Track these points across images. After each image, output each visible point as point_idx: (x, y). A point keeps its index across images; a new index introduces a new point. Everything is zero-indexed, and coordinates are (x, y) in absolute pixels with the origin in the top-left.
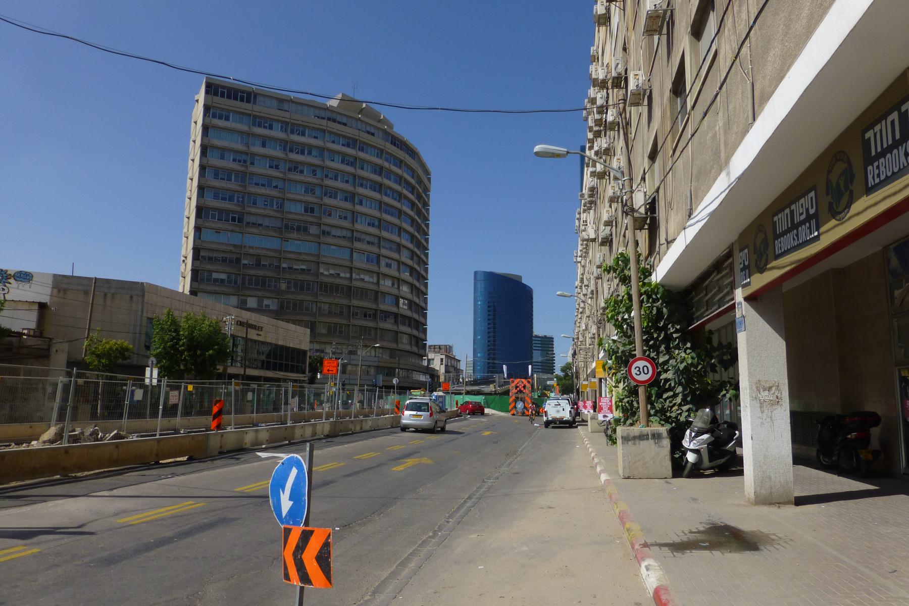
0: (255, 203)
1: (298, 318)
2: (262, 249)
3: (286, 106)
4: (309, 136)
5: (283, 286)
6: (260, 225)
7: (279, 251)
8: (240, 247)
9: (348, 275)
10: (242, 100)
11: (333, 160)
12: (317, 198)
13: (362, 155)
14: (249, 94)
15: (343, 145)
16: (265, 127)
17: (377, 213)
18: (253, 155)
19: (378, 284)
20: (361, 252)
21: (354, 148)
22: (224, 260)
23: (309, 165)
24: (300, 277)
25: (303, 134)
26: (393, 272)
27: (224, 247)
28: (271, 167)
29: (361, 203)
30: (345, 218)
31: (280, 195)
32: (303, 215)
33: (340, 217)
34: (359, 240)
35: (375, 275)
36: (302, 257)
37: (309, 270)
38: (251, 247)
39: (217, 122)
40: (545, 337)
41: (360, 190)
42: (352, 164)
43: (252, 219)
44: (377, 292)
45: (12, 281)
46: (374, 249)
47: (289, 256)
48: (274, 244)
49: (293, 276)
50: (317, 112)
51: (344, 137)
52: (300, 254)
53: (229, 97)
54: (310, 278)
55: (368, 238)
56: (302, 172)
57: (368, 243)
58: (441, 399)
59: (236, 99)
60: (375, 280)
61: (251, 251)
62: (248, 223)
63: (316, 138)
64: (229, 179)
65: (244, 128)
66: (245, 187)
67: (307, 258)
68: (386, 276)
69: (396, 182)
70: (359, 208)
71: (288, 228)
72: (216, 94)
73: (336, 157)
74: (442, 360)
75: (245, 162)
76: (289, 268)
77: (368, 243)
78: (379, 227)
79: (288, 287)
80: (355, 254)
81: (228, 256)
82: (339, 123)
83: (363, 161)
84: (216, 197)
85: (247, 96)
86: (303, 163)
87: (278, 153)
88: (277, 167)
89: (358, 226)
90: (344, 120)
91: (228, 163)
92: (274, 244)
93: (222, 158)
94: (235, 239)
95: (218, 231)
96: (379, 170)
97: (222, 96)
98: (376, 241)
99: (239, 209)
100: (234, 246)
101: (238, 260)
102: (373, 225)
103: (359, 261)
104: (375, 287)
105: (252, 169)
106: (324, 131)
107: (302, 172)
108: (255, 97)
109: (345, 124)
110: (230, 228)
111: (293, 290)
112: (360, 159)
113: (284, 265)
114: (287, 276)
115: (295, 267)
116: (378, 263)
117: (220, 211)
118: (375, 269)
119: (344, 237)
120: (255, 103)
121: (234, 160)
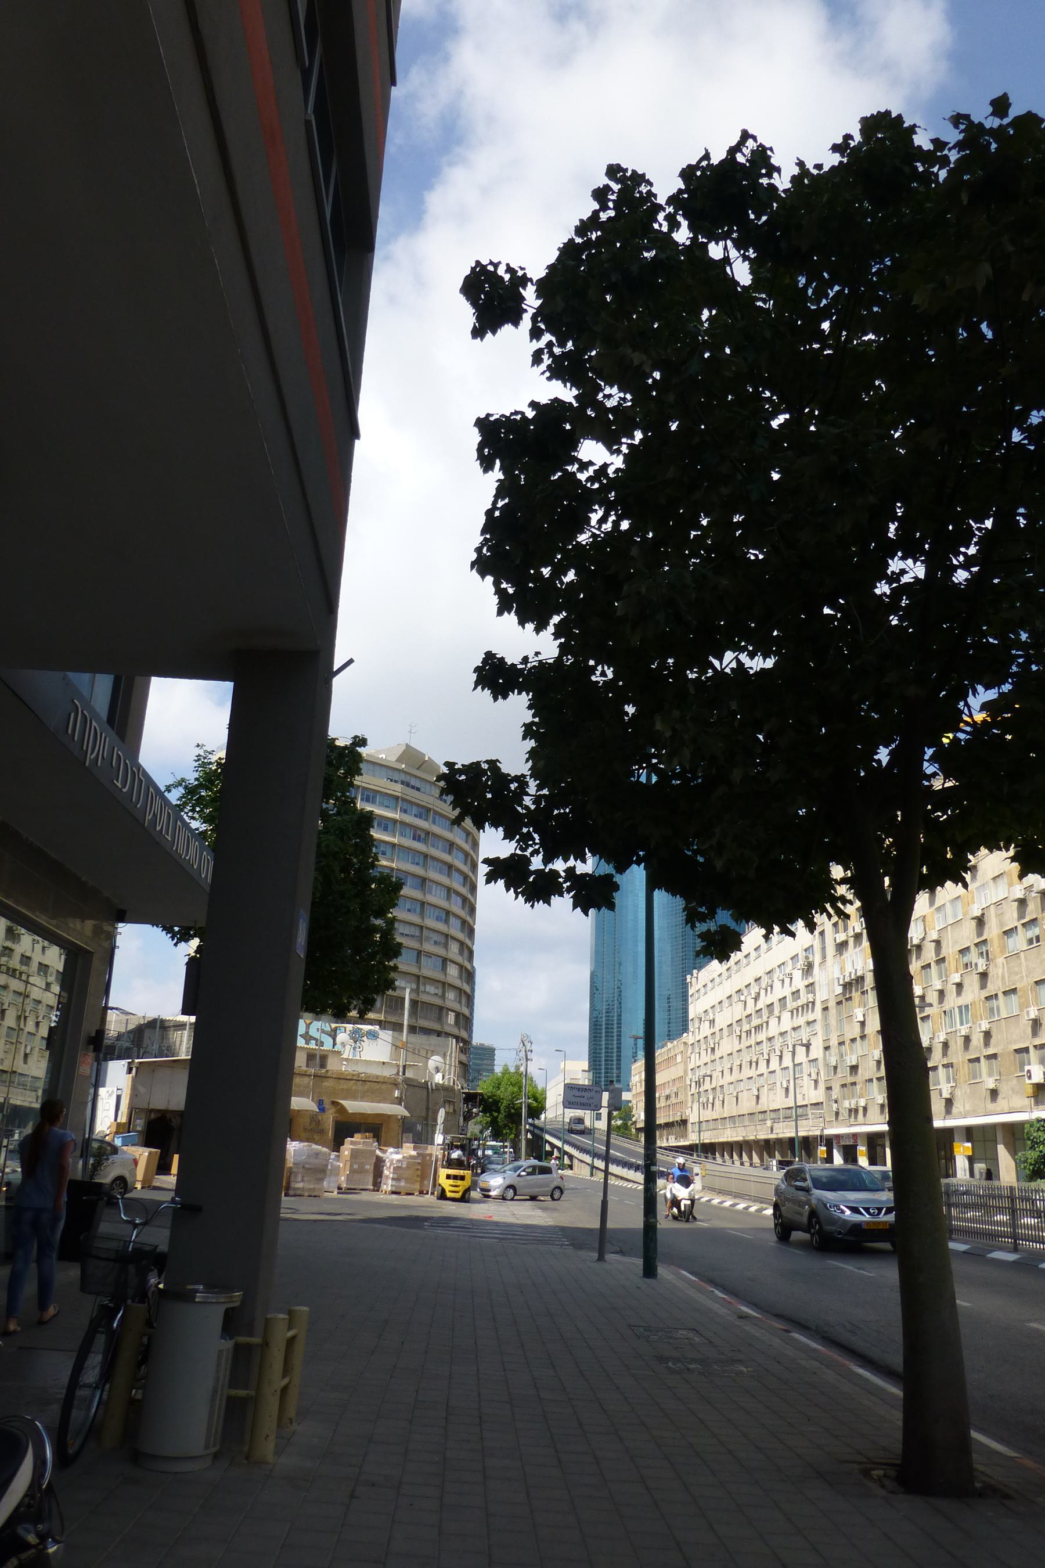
13: (436, 829)
15: (415, 816)
17: (444, 904)
19: (443, 997)
20: (429, 955)
21: (426, 820)
25: (374, 802)
26: (458, 983)
29: (430, 893)
30: (415, 911)
33: (409, 910)
34: (428, 939)
35: (440, 985)
41: (433, 875)
42: (425, 841)
44: (441, 1009)
45: (365, 1038)
46: (441, 951)
50: (390, 773)
51: (418, 805)
55: (435, 937)
57: (435, 943)
60: (440, 992)
68: (453, 987)
69: (444, 851)
70: (430, 898)
73: (408, 830)
77: (435, 943)
78: (447, 922)
82: (413, 787)
83: (435, 835)
89: (430, 922)
90: (418, 784)
96: (451, 846)
98: (441, 939)
102: (441, 920)
103: (429, 969)
104: (438, 1001)
106: (397, 798)
109: (418, 789)
112: (433, 834)
116: (444, 968)
118: (440, 977)
119: (413, 936)
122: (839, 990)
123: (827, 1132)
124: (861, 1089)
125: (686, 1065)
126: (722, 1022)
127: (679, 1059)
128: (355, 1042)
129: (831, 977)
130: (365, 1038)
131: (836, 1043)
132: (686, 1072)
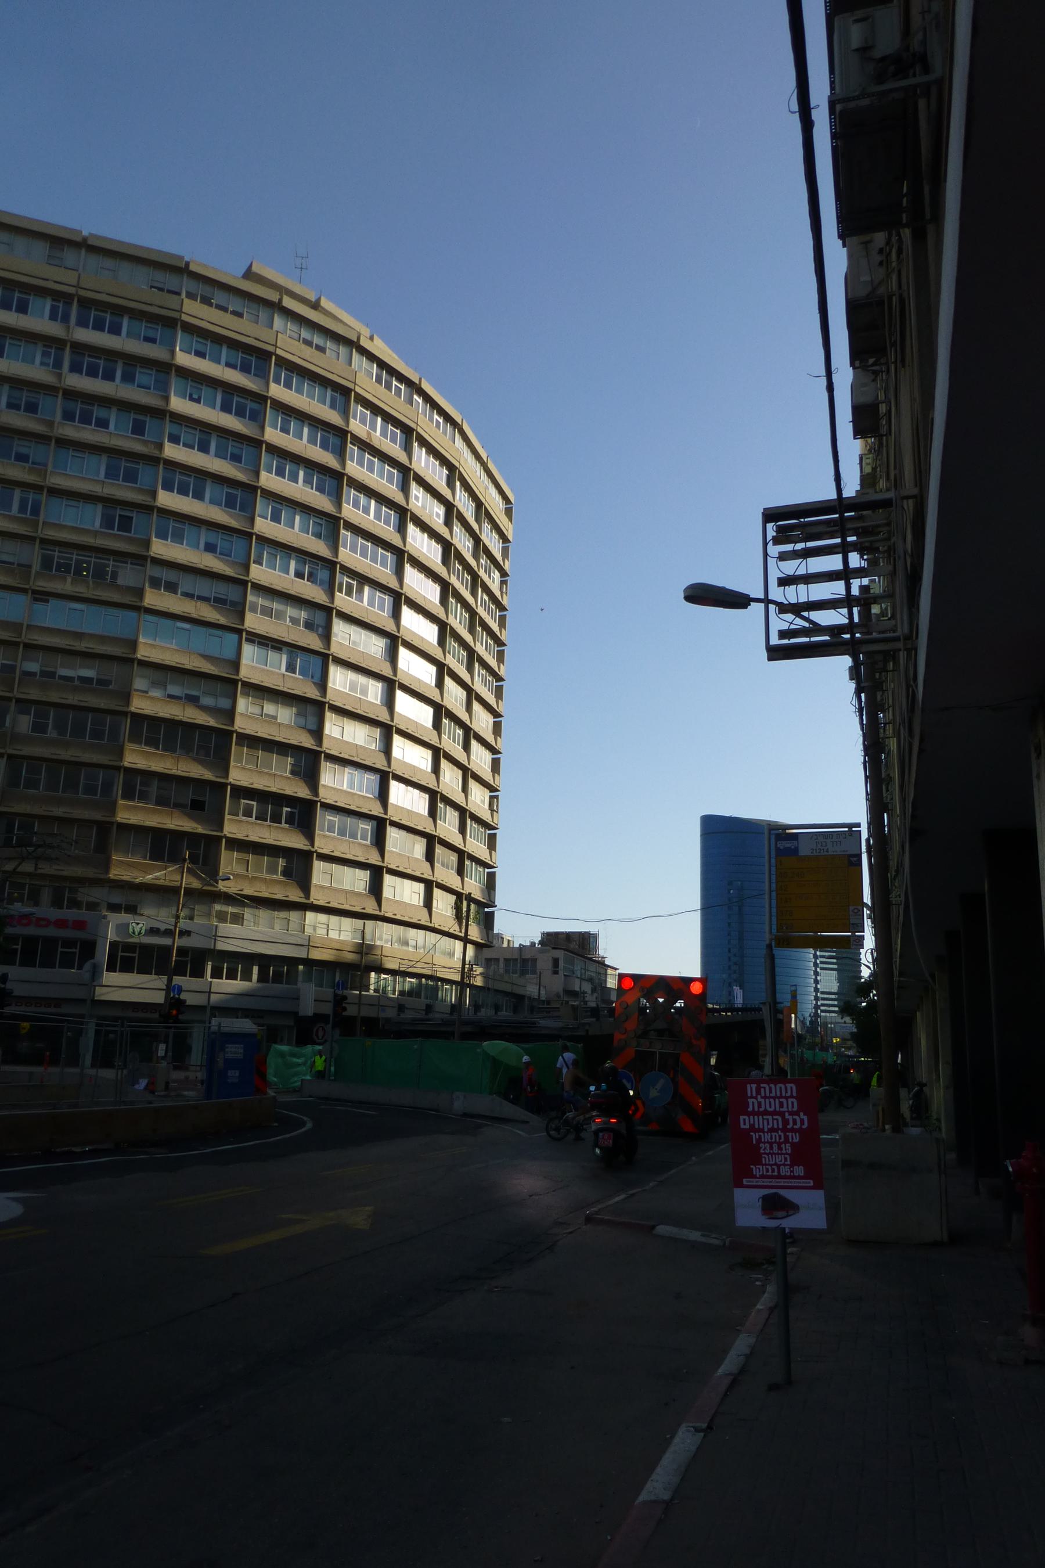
1: (59, 811)
3: (70, 257)
4: (129, 335)
5: (24, 723)
9: (224, 703)
11: (198, 401)
12: (140, 491)
15: (228, 365)
23: (125, 406)
24: (73, 699)
25: (115, 330)
28: (11, 406)
31: (31, 478)
36: (82, 646)
37: (100, 682)
49: (54, 697)
50: (160, 277)
51: (234, 345)
52: (79, 636)
54: (102, 703)
63: (152, 340)
73: (206, 391)
74: (556, 962)
79: (39, 727)
86: (106, 402)
87: (36, 371)
88: (32, 408)
107: (103, 424)
111: (51, 733)
113: (33, 667)
114: (34, 694)
115: (63, 672)
119: (217, 600)
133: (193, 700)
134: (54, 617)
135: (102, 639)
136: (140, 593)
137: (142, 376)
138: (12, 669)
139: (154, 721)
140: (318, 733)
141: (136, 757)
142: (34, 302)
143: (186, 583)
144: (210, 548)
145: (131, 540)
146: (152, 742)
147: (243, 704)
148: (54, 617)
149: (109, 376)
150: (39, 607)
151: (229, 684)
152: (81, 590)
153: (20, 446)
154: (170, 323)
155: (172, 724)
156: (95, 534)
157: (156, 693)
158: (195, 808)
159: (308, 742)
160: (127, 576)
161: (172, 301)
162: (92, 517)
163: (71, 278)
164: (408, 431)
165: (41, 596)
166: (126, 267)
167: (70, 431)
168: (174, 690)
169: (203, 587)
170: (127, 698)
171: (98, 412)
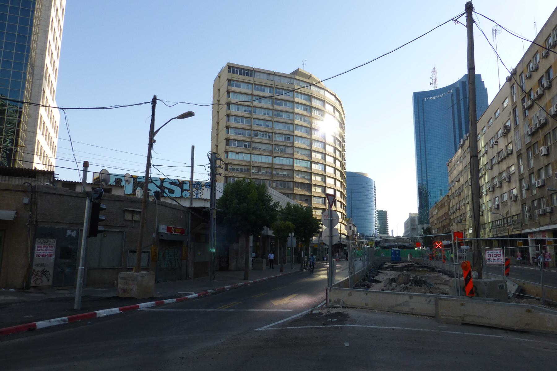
0: (257, 136)
2: (262, 163)
3: (271, 77)
6: (260, 149)
7: (272, 164)
8: (250, 162)
9: (309, 177)
10: (247, 75)
12: (291, 131)
14: (251, 71)
16: (261, 91)
18: (255, 107)
22: (241, 170)
24: (284, 179)
27: (240, 163)
32: (283, 142)
36: (284, 167)
37: (288, 175)
38: (256, 162)
39: (234, 89)
40: (382, 211)
43: (255, 145)
45: (204, 188)
47: (277, 167)
48: (268, 160)
49: (280, 179)
50: (289, 80)
52: (283, 165)
53: (240, 74)
54: (289, 180)
56: (282, 116)
58: (397, 252)
59: (244, 75)
61: (256, 165)
62: (253, 148)
64: (242, 122)
65: (249, 92)
66: (251, 126)
67: (287, 168)
71: (275, 150)
72: (233, 72)
73: (300, 106)
75: (250, 111)
76: (277, 174)
79: (277, 186)
80: (313, 165)
81: (243, 168)
84: (236, 133)
85: (251, 72)
87: (268, 106)
91: (241, 112)
92: (268, 160)
93: (238, 110)
94: (247, 157)
95: (237, 153)
97: (237, 73)
99: (248, 140)
100: (247, 162)
101: (249, 170)
105: (254, 116)
108: (254, 73)
110: (244, 151)
111: (280, 187)
113: (274, 172)
114: (276, 179)
115: (280, 173)
117: (238, 140)
120: (254, 77)
121: (245, 111)
122: (528, 139)
123: (523, 232)
124: (547, 201)
125: (449, 205)
126: (462, 181)
127: (446, 204)
128: (197, 190)
129: (522, 134)
130: (204, 188)
131: (528, 175)
132: (449, 210)
133: (304, 177)
134: (278, 161)
135: (288, 165)
136: (293, 154)
137: (289, 104)
138: (272, 173)
139: (298, 183)
140: (325, 182)
141: (297, 191)
142: (266, 89)
143: (301, 152)
144: (304, 143)
145: (290, 143)
146: (298, 187)
147: (313, 178)
148: (278, 161)
149: (282, 105)
150: (274, 159)
151: (310, 174)
152: (282, 155)
153: (267, 123)
154: (293, 91)
155: (301, 183)
156: (283, 142)
157: (297, 177)
158: (306, 200)
159: (324, 185)
160: (289, 151)
161: (291, 86)
162: (281, 139)
163: (272, 83)
164: (334, 107)
165: (275, 157)
166: (282, 78)
167: (276, 119)
168: (300, 175)
169: (304, 152)
170: (293, 178)
171: (281, 113)
